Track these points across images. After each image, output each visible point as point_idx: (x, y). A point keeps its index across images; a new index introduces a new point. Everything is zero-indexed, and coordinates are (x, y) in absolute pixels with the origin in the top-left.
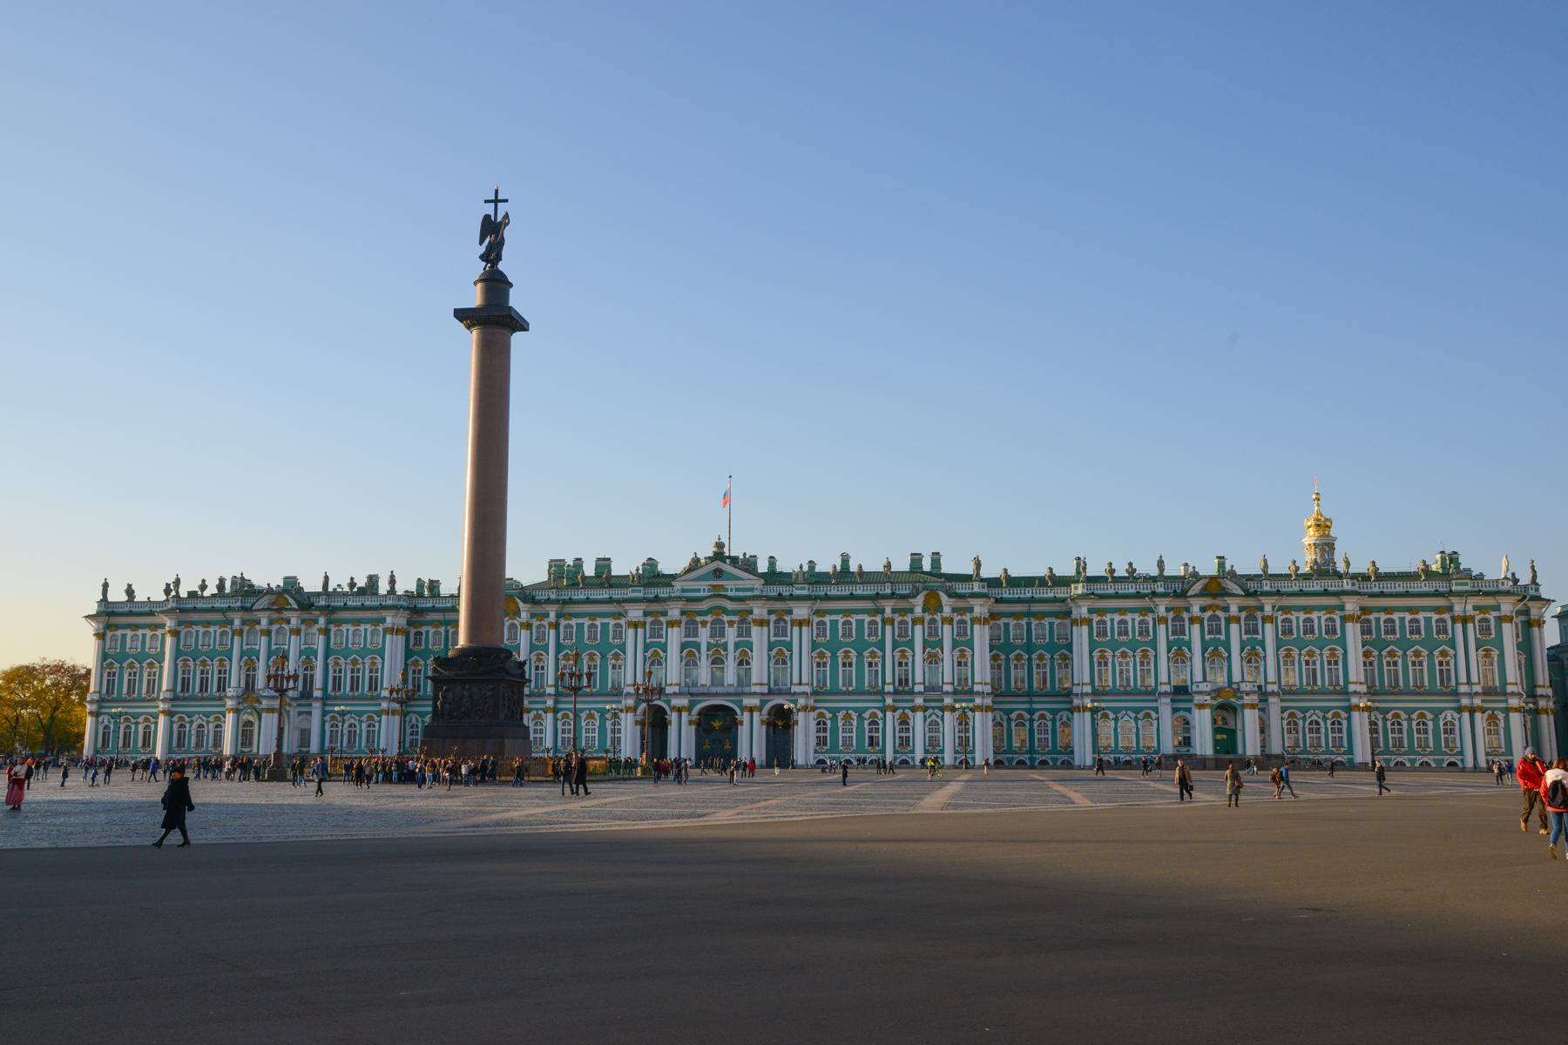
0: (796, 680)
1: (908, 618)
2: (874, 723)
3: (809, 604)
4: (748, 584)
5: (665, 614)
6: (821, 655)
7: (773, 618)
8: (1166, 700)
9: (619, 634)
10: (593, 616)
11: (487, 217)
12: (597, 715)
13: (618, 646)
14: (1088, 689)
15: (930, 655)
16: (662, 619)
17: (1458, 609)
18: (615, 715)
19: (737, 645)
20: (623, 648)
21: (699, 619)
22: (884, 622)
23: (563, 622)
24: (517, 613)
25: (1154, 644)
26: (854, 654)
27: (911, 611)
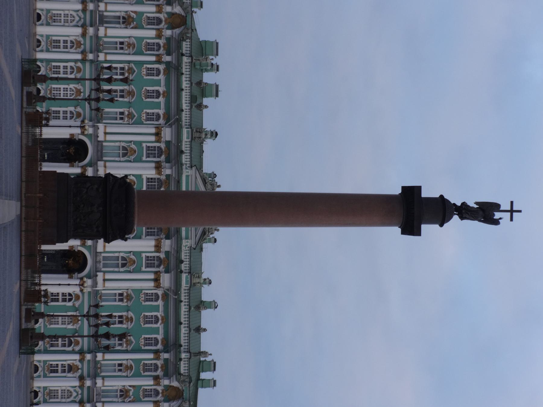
0: (108, 276)
1: (159, 372)
5: (168, 161)
6: (129, 298)
7: (162, 256)
9: (150, 117)
10: (167, 95)
11: (496, 207)
13: (140, 116)
15: (127, 391)
16: (163, 157)
20: (139, 123)
23: (162, 67)
24: (172, 27)
27: (167, 375)
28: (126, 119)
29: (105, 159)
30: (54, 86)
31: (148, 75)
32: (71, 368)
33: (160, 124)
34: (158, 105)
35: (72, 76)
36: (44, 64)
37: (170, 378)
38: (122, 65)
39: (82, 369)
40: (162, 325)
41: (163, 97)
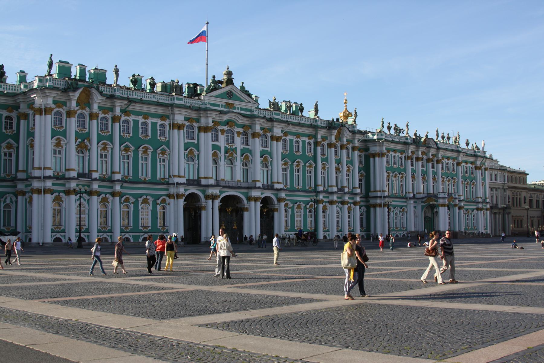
1: (325, 143)
2: (310, 211)
3: (283, 126)
4: (248, 106)
5: (198, 120)
6: (286, 164)
8: (412, 201)
10: (146, 116)
12: (151, 200)
14: (386, 194)
16: (196, 125)
17: (478, 163)
18: (164, 201)
19: (243, 152)
21: (220, 128)
22: (316, 144)
23: (123, 118)
25: (405, 170)
26: (302, 164)
28: (165, 156)
29: (196, 178)
30: (140, 225)
31: (128, 132)
32: (324, 212)
33: (170, 125)
34: (154, 124)
35: (132, 206)
36: (123, 234)
37: (331, 135)
38: (121, 157)
39: (326, 202)
40: (301, 138)
41: (147, 118)
